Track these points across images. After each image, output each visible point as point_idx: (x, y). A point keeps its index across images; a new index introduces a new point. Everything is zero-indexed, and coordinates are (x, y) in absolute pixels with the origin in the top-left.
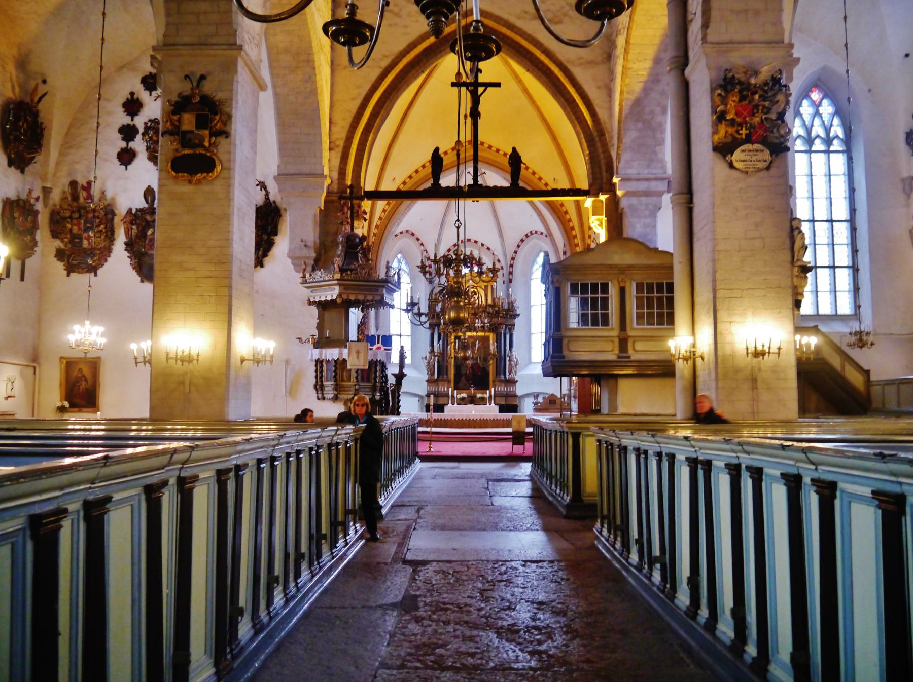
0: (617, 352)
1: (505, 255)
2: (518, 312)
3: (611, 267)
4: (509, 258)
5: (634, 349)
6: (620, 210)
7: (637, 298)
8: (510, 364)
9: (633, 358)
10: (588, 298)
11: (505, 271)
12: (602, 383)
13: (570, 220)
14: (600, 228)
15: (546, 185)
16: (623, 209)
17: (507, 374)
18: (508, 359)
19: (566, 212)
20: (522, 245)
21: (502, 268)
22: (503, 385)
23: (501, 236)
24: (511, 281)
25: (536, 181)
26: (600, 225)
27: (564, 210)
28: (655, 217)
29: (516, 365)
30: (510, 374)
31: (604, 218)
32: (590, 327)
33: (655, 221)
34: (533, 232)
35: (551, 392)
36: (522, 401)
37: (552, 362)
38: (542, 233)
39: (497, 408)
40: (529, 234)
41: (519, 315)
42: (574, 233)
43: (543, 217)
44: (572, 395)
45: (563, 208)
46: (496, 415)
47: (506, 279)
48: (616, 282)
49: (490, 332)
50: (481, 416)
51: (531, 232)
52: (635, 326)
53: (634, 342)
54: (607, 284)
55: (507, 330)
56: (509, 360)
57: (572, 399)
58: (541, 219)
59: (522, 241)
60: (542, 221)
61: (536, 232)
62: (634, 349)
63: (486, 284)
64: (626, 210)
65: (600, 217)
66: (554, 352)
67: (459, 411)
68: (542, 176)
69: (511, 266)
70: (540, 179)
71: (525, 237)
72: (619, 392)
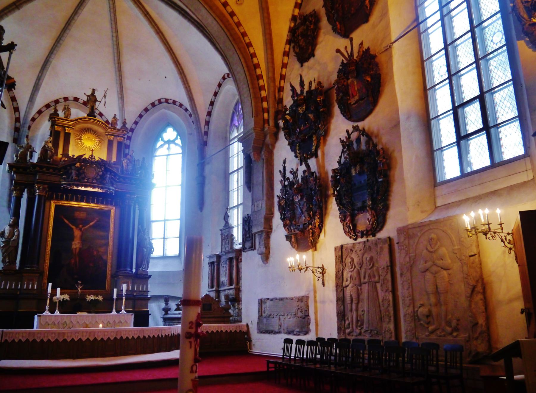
13: (254, 55)
19: (249, 45)
22: (130, 281)
27: (247, 41)
34: (163, 100)
38: (174, 102)
39: (131, 318)
40: (157, 103)
42: (258, 72)
43: (185, 76)
45: (246, 38)
46: (130, 331)
49: (111, 204)
50: (118, 332)
51: (160, 101)
55: (137, 206)
59: (146, 110)
61: (167, 101)
63: (111, 137)
67: (65, 324)
71: (150, 106)
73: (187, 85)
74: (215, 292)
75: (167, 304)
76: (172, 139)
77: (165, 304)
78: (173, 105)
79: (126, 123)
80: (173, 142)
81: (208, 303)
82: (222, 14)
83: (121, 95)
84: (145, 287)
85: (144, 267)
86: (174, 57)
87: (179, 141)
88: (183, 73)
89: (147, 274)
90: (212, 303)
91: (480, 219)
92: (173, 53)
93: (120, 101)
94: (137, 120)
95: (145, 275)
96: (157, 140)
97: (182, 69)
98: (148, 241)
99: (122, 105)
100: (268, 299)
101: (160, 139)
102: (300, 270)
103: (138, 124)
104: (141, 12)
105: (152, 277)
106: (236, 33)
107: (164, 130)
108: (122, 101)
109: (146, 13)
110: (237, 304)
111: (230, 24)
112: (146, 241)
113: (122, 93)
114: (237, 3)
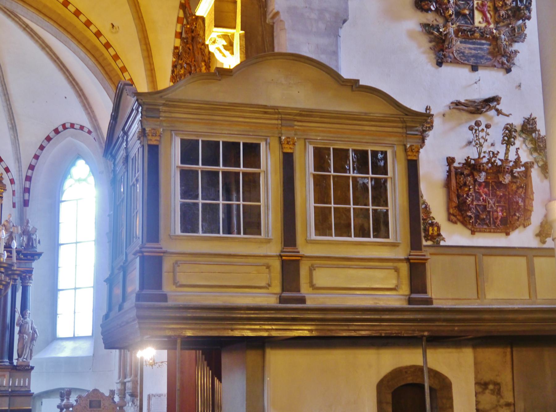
0: (277, 288)
1: (18, 160)
2: (39, 249)
3: (266, 110)
4: (25, 167)
5: (312, 286)
6: (268, 20)
7: (315, 176)
8: (21, 338)
9: (309, 304)
10: (217, 173)
11: (17, 187)
12: (226, 360)
14: (227, 53)
15: (98, 34)
16: (277, 13)
17: (15, 356)
18: (17, 329)
20: (48, 147)
21: (12, 181)
22: (7, 374)
23: (13, 127)
24: (26, 203)
25: (81, 27)
26: (230, 46)
28: (337, 36)
29: (33, 339)
30: (19, 356)
31: (237, 33)
32: (221, 234)
33: (337, 45)
34: (68, 125)
35: (90, 388)
36: (38, 404)
37: (138, 307)
38: (82, 128)
40: (60, 129)
41: (40, 255)
43: (86, 98)
44: (128, 391)
45: (126, 74)
47: (18, 199)
48: (275, 143)
51: (64, 126)
52: (314, 237)
53: (311, 269)
54: (258, 146)
56: (20, 332)
57: (128, 397)
58: (82, 102)
59: (48, 139)
60: (84, 106)
61: (72, 126)
62: (312, 286)
64: (283, 16)
65: (229, 31)
66: (142, 286)
68: (91, 20)
69: (28, 179)
70: (88, 24)
71: (53, 133)
72: (267, 379)
73: (89, 110)
74: (120, 384)
75: (62, 400)
76: (83, 177)
77: (61, 400)
78: (81, 131)
79: (3, 178)
80: (85, 180)
81: (97, 399)
82: (95, 47)
83: (12, 124)
84: (22, 382)
85: (25, 357)
86: (68, 75)
87: (91, 179)
88: (84, 95)
89: (29, 366)
90: (102, 400)
91: (166, 341)
92: (68, 70)
93: (12, 132)
94: (38, 154)
95: (26, 366)
96: (64, 178)
97: (81, 90)
98: (30, 325)
99: (15, 137)
100: (153, 395)
101: (69, 176)
102: (152, 366)
103: (40, 158)
104: (19, 26)
105: (34, 368)
106: (114, 69)
107: (73, 164)
108: (13, 131)
109: (24, 26)
110: (136, 400)
111: (105, 59)
112: (27, 326)
113: (13, 122)
114: (112, 32)
